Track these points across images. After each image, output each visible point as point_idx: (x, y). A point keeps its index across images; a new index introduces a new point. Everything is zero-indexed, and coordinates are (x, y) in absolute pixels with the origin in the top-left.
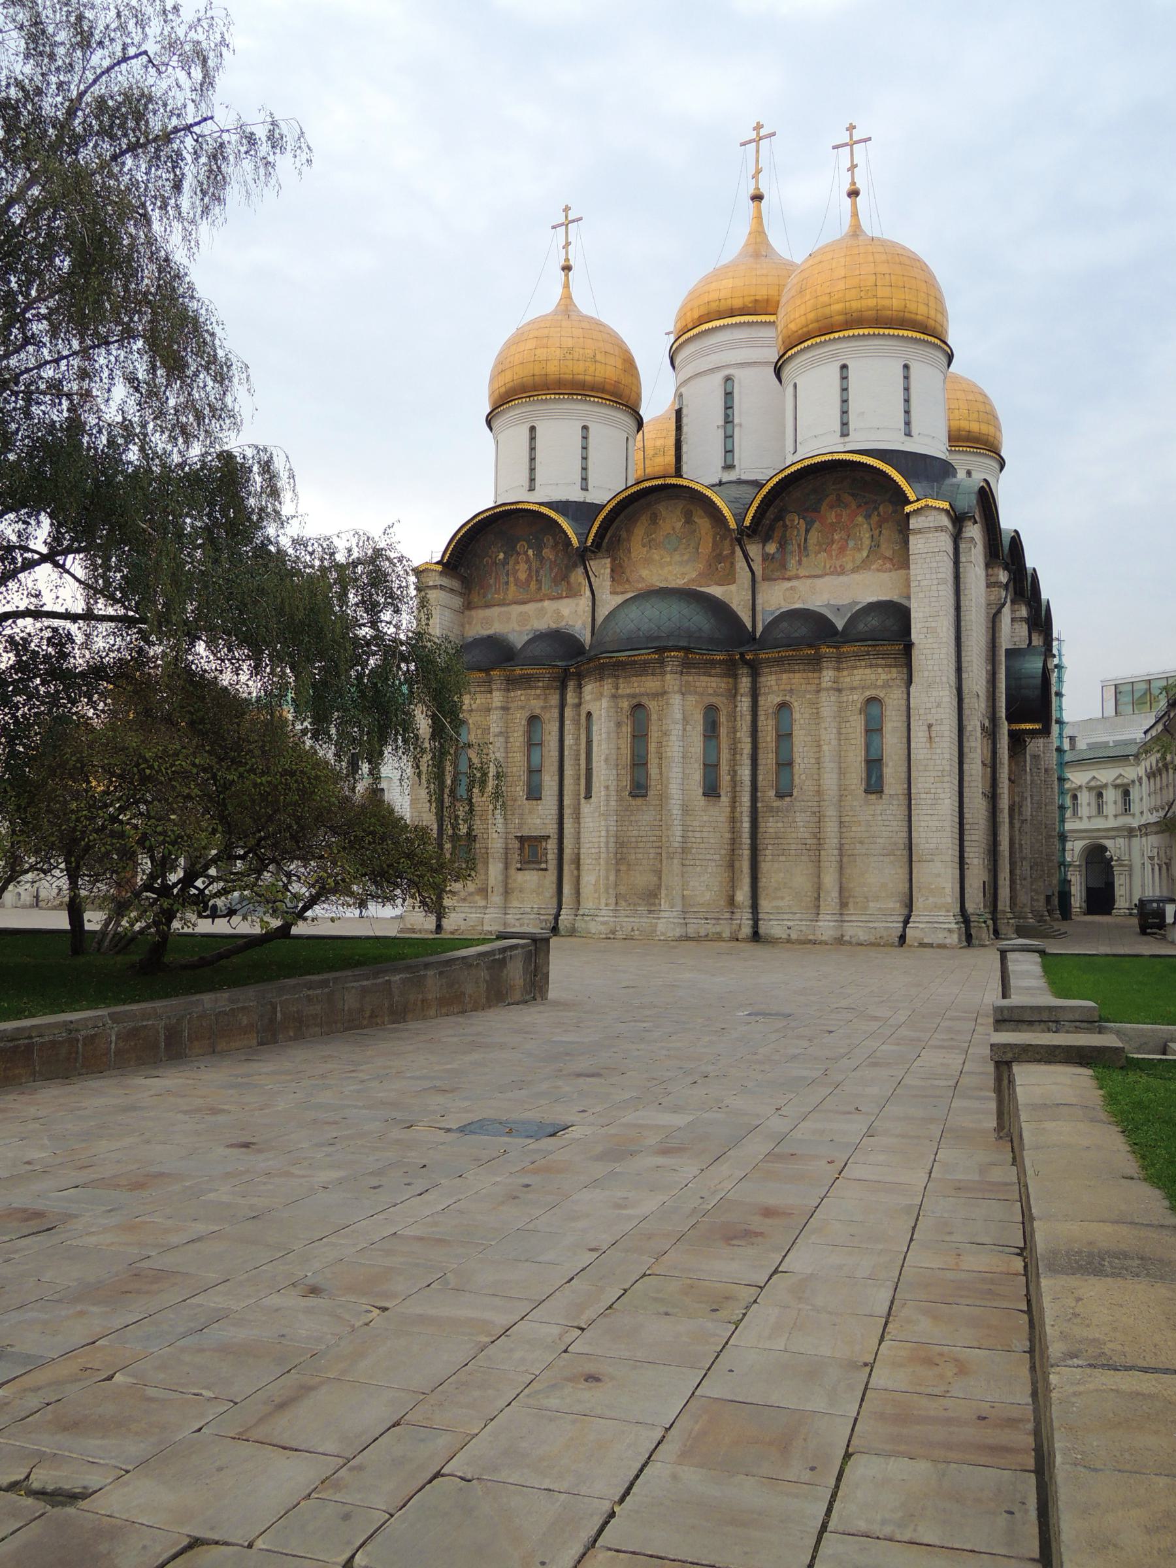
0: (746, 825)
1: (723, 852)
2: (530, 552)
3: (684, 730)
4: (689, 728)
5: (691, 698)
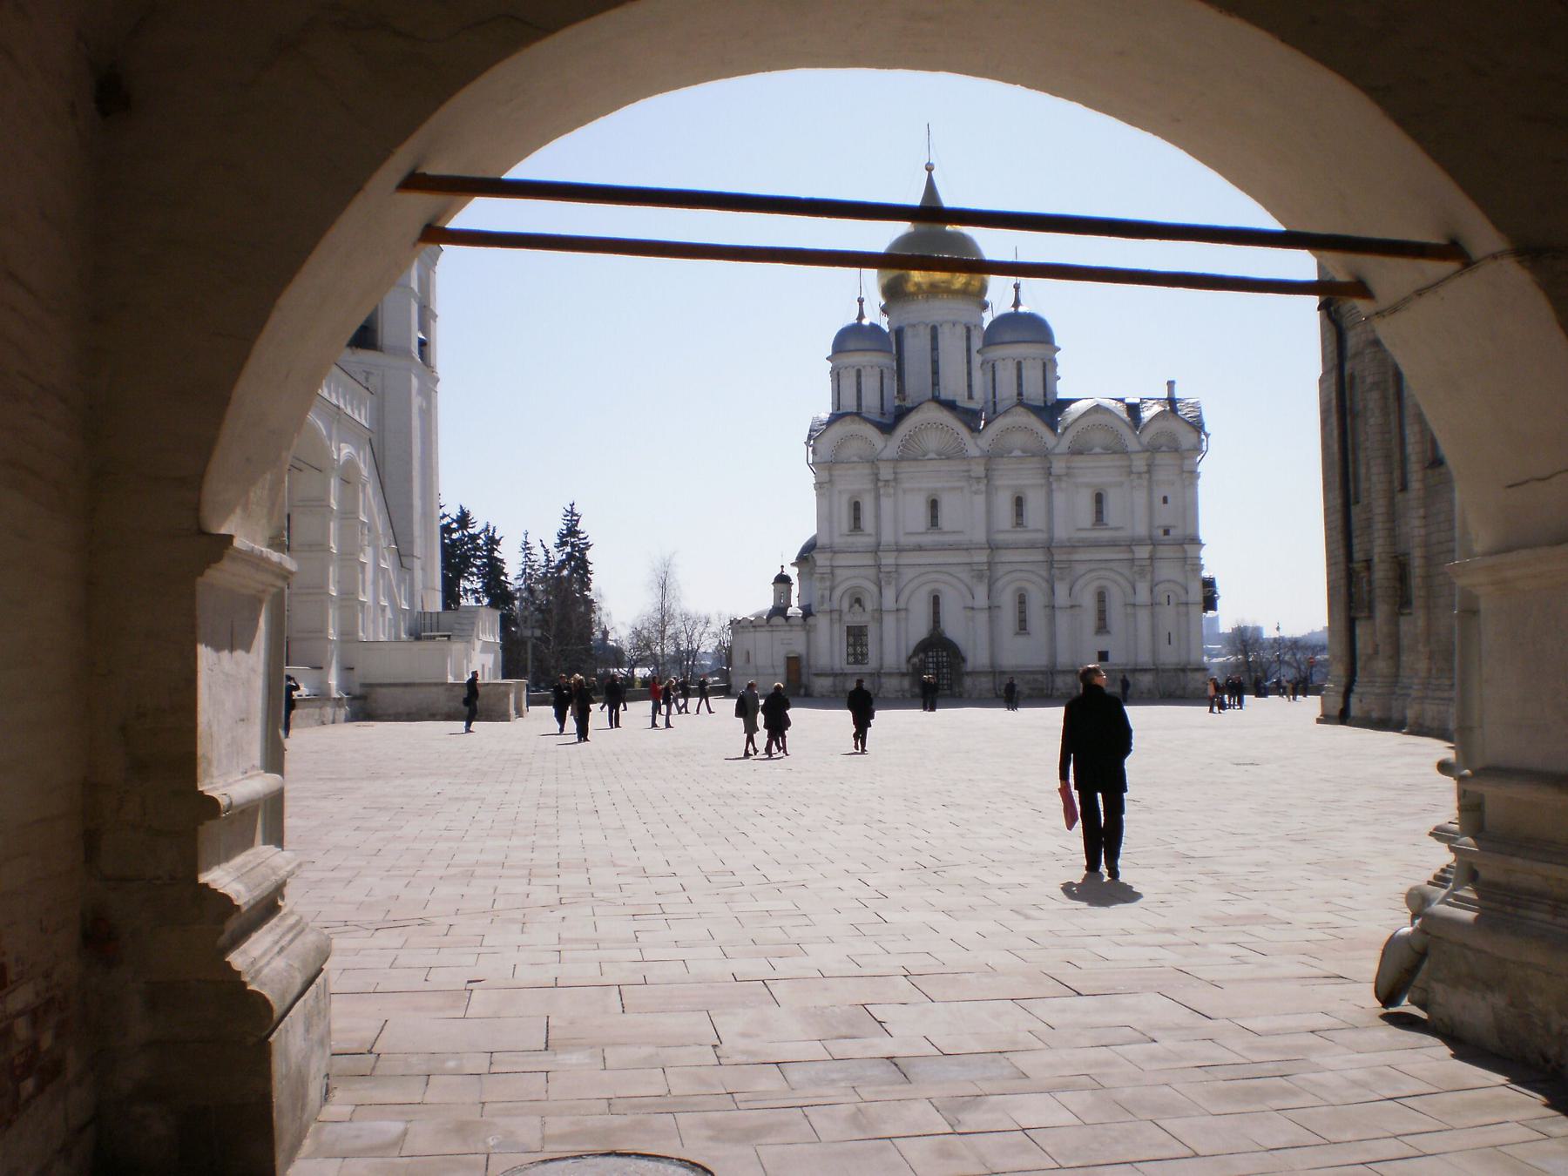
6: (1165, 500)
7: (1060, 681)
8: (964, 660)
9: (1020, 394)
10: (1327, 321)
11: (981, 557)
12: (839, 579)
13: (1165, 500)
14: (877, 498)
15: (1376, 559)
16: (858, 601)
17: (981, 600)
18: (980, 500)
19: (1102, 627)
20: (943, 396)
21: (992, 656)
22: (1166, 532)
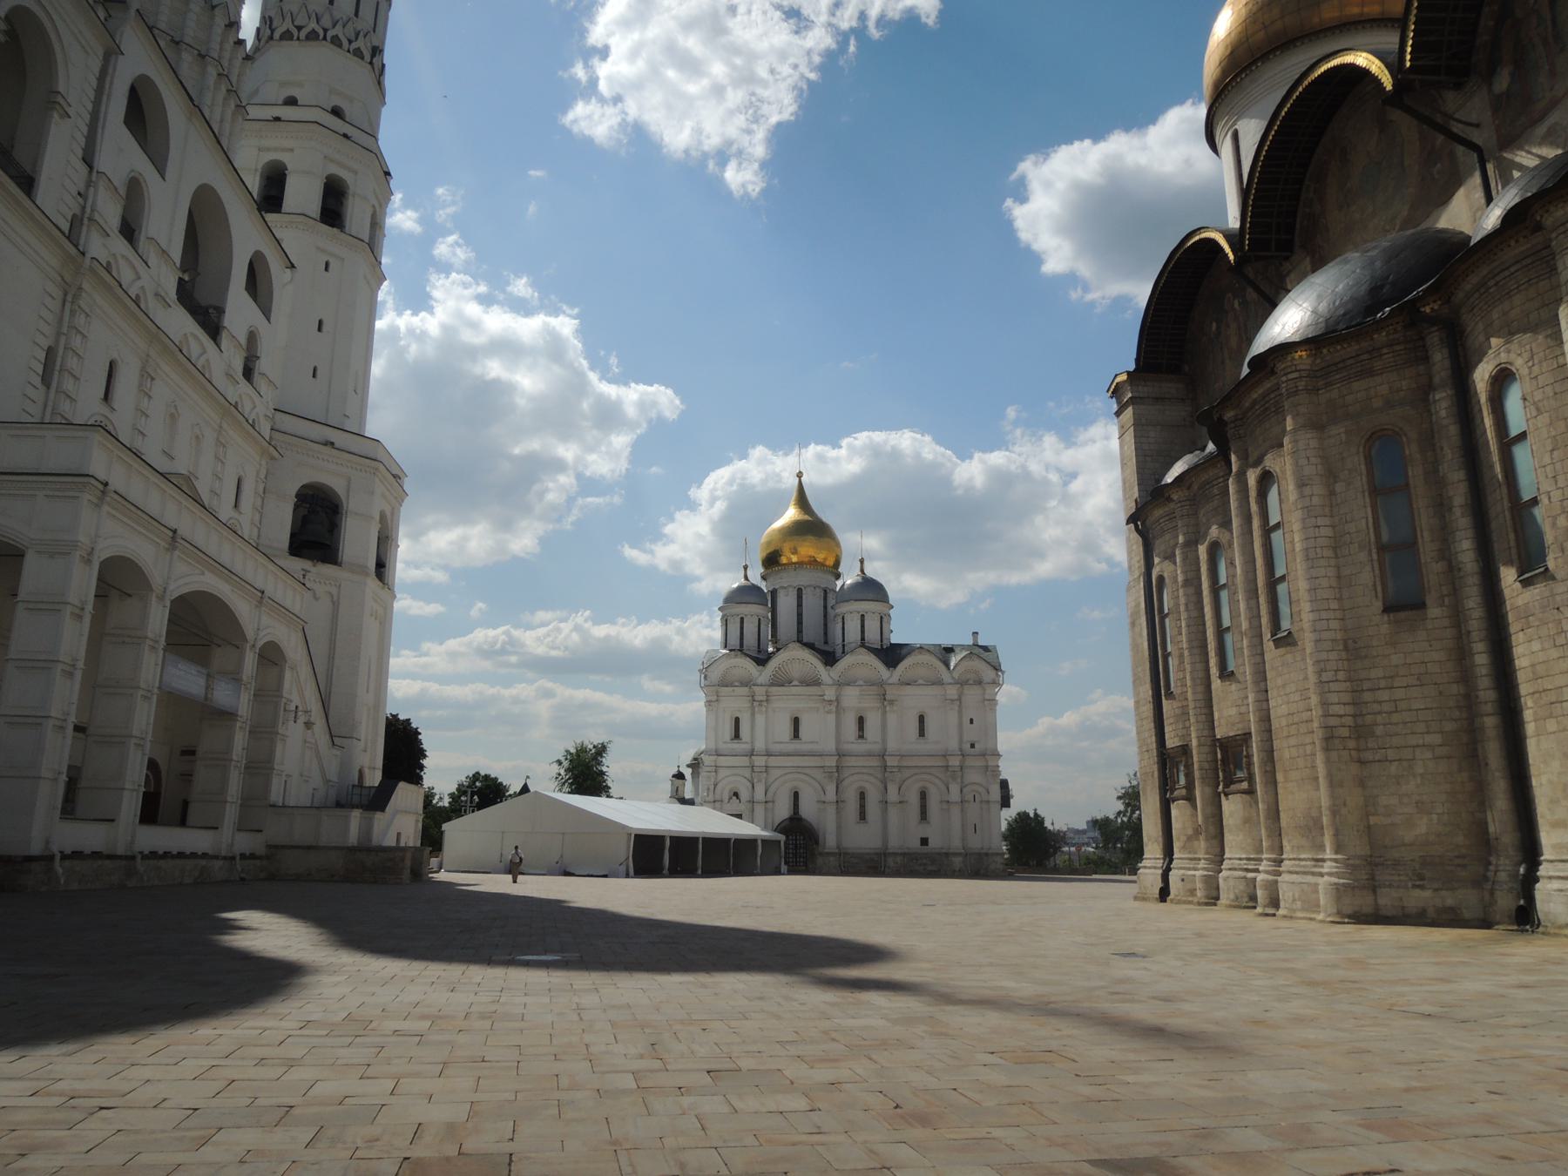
0: (1481, 659)
1: (1449, 726)
2: (1236, 305)
3: (1332, 493)
4: (1339, 487)
5: (1338, 431)
6: (971, 721)
7: (890, 861)
8: (817, 842)
9: (863, 639)
10: (1135, 535)
13: (971, 721)
14: (753, 714)
15: (1194, 743)
16: (736, 794)
17: (831, 795)
18: (832, 718)
19: (924, 815)
20: (805, 640)
22: (973, 746)
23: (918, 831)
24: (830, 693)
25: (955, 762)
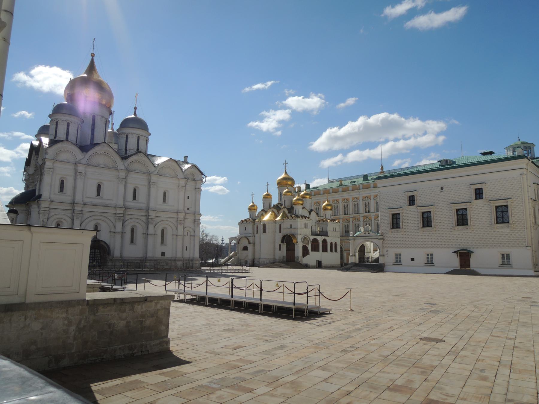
8: (109, 254)
9: (138, 149)
11: (120, 211)
12: (52, 214)
14: (75, 180)
17: (119, 229)
21: (121, 253)
22: (188, 209)
23: (160, 249)
24: (122, 174)
25: (181, 216)
